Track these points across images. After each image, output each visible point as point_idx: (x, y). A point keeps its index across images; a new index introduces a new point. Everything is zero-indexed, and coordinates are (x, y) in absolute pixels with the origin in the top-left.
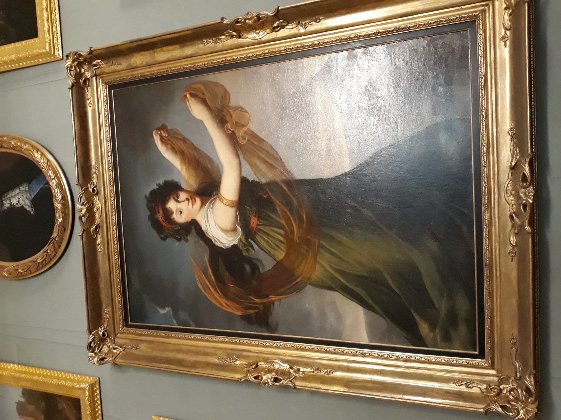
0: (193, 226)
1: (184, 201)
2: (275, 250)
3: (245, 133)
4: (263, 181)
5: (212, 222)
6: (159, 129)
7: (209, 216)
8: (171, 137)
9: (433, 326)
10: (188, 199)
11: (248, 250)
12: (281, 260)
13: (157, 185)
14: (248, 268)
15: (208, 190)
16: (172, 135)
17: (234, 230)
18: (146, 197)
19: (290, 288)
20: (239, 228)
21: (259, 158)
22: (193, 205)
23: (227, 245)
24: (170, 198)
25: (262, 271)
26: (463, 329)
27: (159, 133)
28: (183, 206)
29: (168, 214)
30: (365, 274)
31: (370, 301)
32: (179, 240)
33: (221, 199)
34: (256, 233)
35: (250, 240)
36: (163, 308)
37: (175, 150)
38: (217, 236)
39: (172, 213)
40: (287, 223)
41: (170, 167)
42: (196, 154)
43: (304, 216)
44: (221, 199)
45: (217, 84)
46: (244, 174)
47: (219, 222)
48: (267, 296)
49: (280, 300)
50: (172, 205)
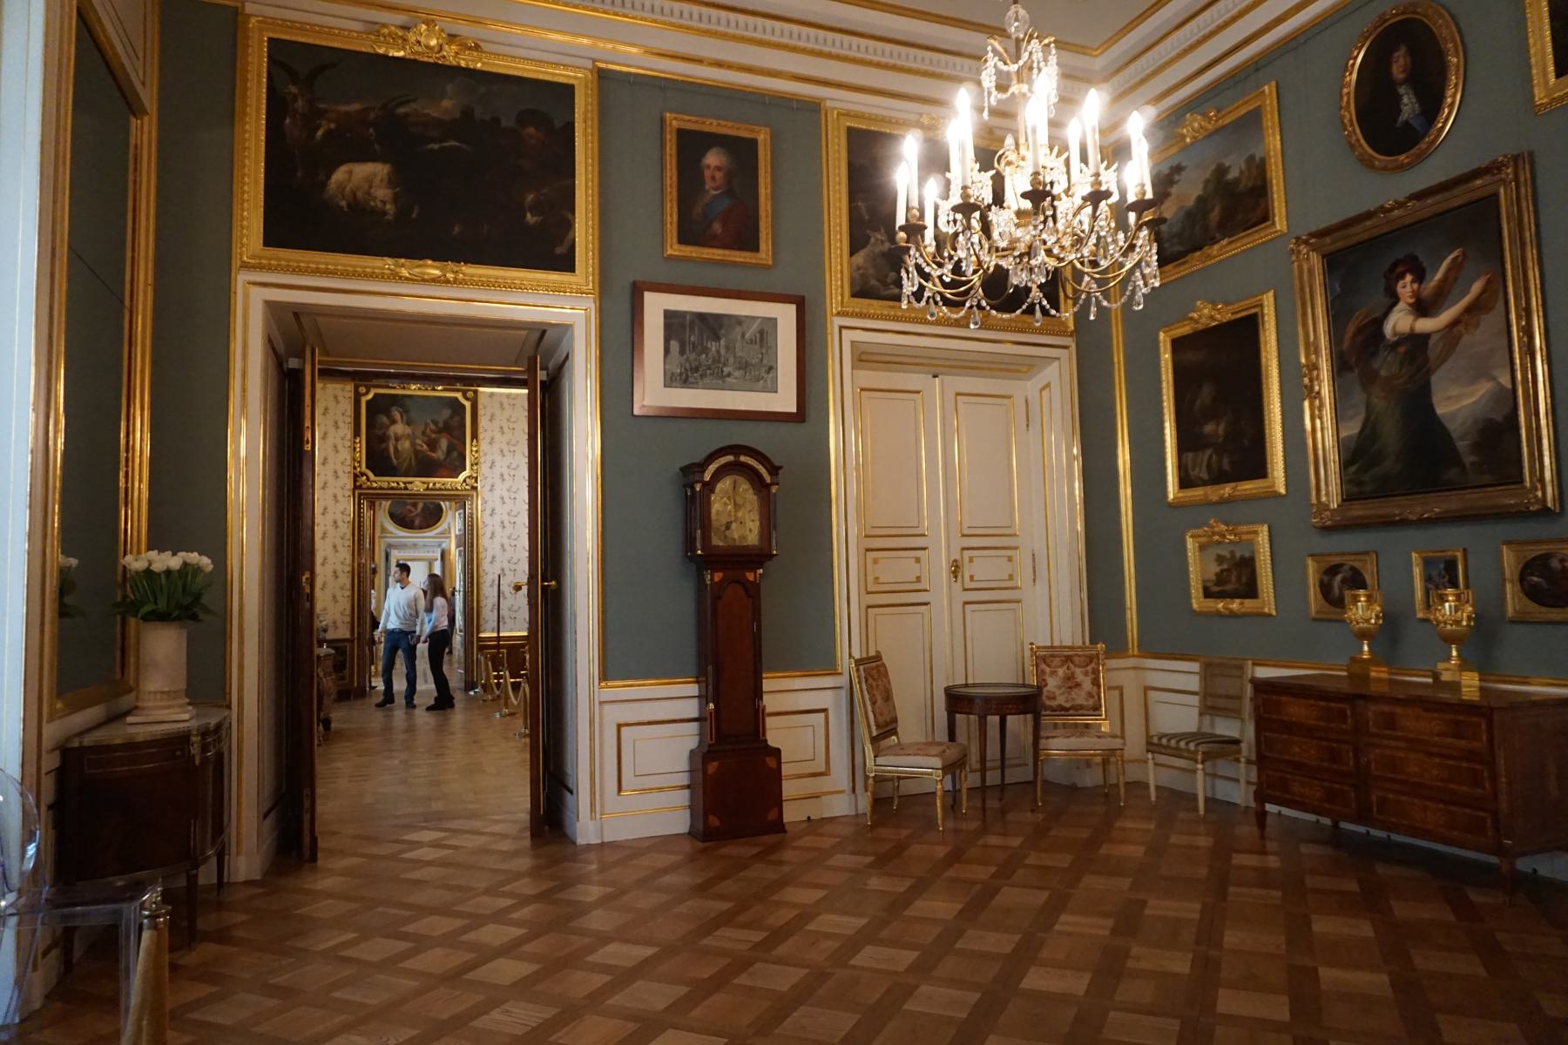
0: (1395, 300)
9: (1355, 473)
15: (1422, 308)
26: (1355, 490)
28: (1408, 288)
29: (1402, 276)
37: (1449, 270)
47: (1399, 321)
50: (1409, 278)
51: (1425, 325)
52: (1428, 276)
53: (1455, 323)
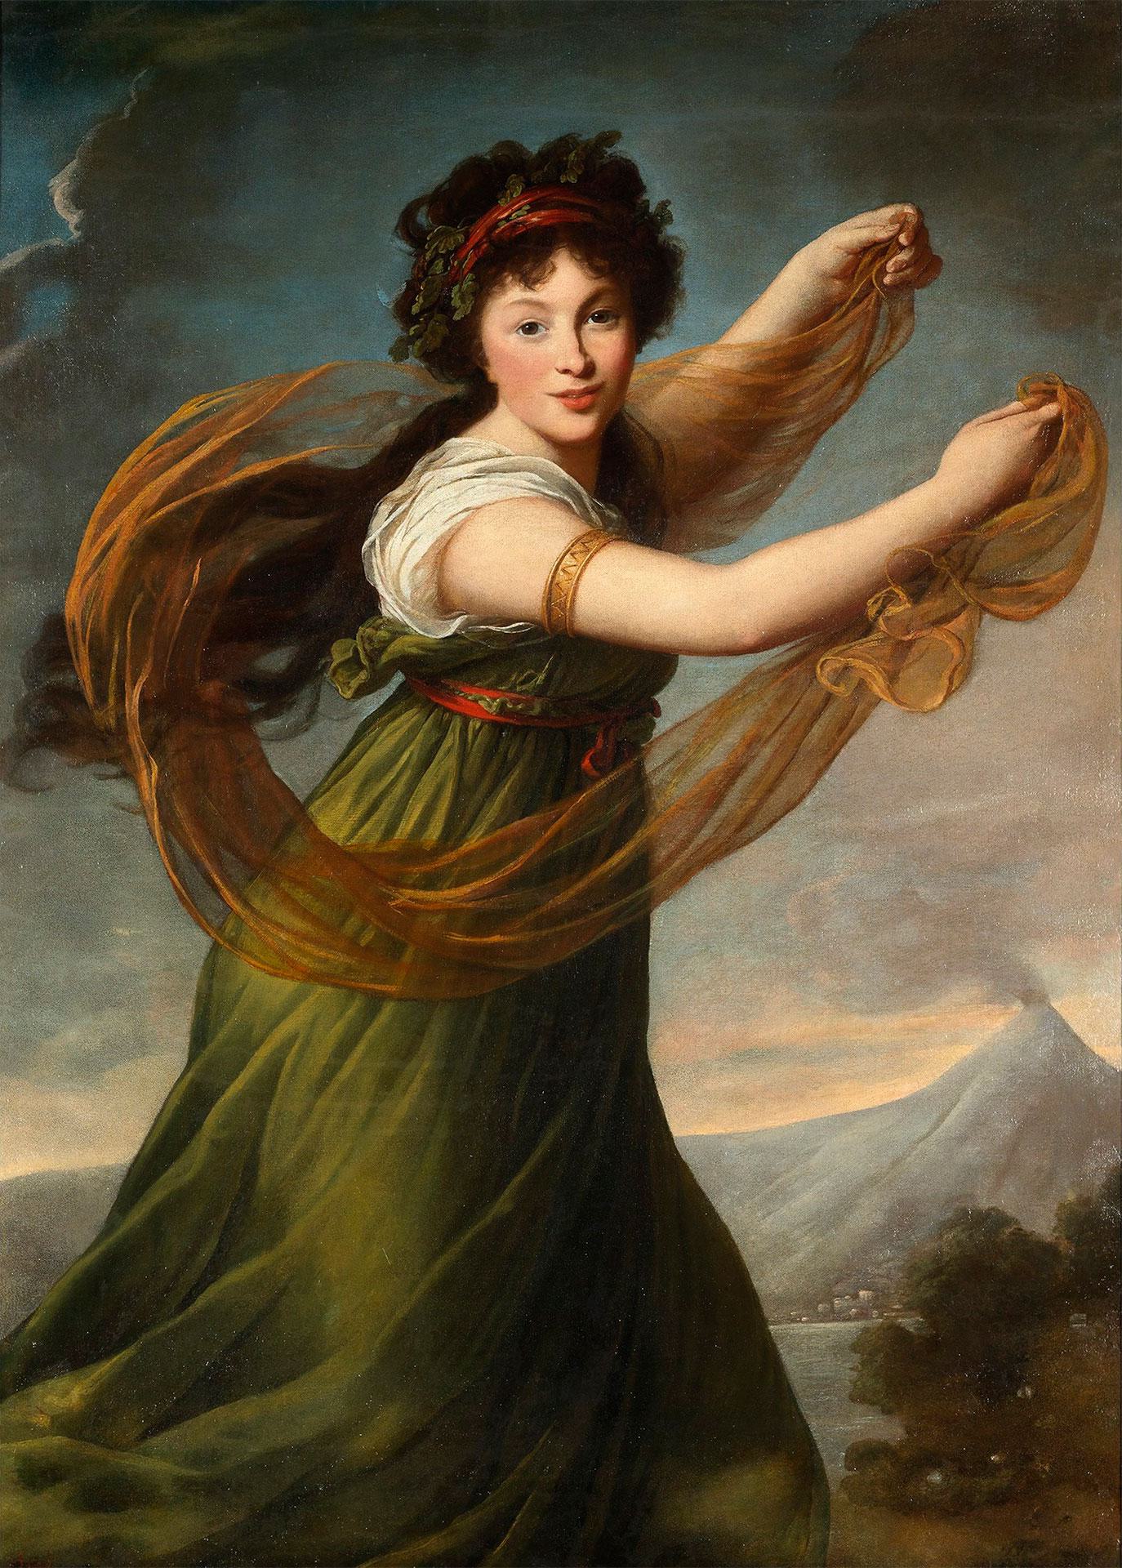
1: (582, 350)
2: (356, 802)
3: (862, 685)
4: (655, 761)
5: (482, 492)
6: (920, 236)
7: (508, 478)
8: (878, 305)
10: (588, 371)
11: (354, 663)
12: (310, 824)
13: (664, 205)
14: (276, 661)
15: (631, 482)
16: (885, 308)
17: (444, 605)
18: (610, 138)
19: (195, 860)
20: (454, 626)
21: (752, 743)
22: (563, 395)
23: (376, 561)
24: (597, 271)
25: (265, 727)
27: (902, 239)
29: (523, 256)
30: (263, 1180)
31: (156, 1195)
32: (403, 310)
33: (584, 547)
34: (430, 707)
35: (399, 678)
36: (77, 198)
37: (818, 318)
38: (418, 509)
39: (529, 282)
40: (469, 855)
41: (745, 288)
42: (792, 429)
43: (496, 938)
44: (584, 547)
45: (1082, 559)
46: (686, 664)
47: (476, 530)
48: (154, 745)
49: (144, 812)
50: (567, 281)
51: (638, 591)
52: (690, 311)
53: (836, 624)
